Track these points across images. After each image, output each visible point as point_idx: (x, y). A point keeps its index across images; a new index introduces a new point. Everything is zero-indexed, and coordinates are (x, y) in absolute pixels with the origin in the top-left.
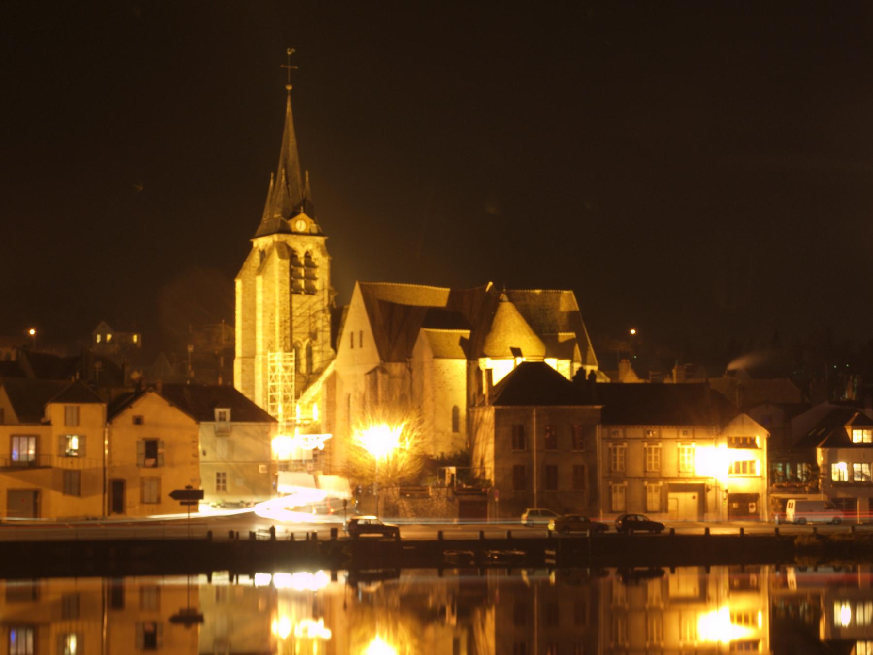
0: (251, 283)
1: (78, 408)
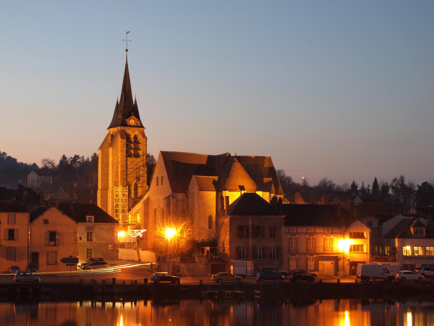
0: (106, 151)
1: (15, 215)
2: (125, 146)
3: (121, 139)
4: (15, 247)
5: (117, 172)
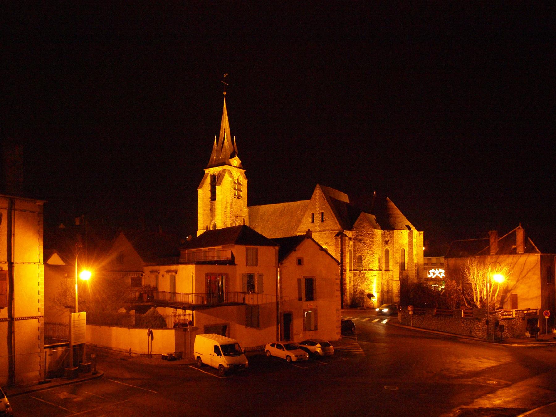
0: (206, 191)
1: (257, 249)
3: (230, 178)
4: (259, 305)
5: (226, 212)
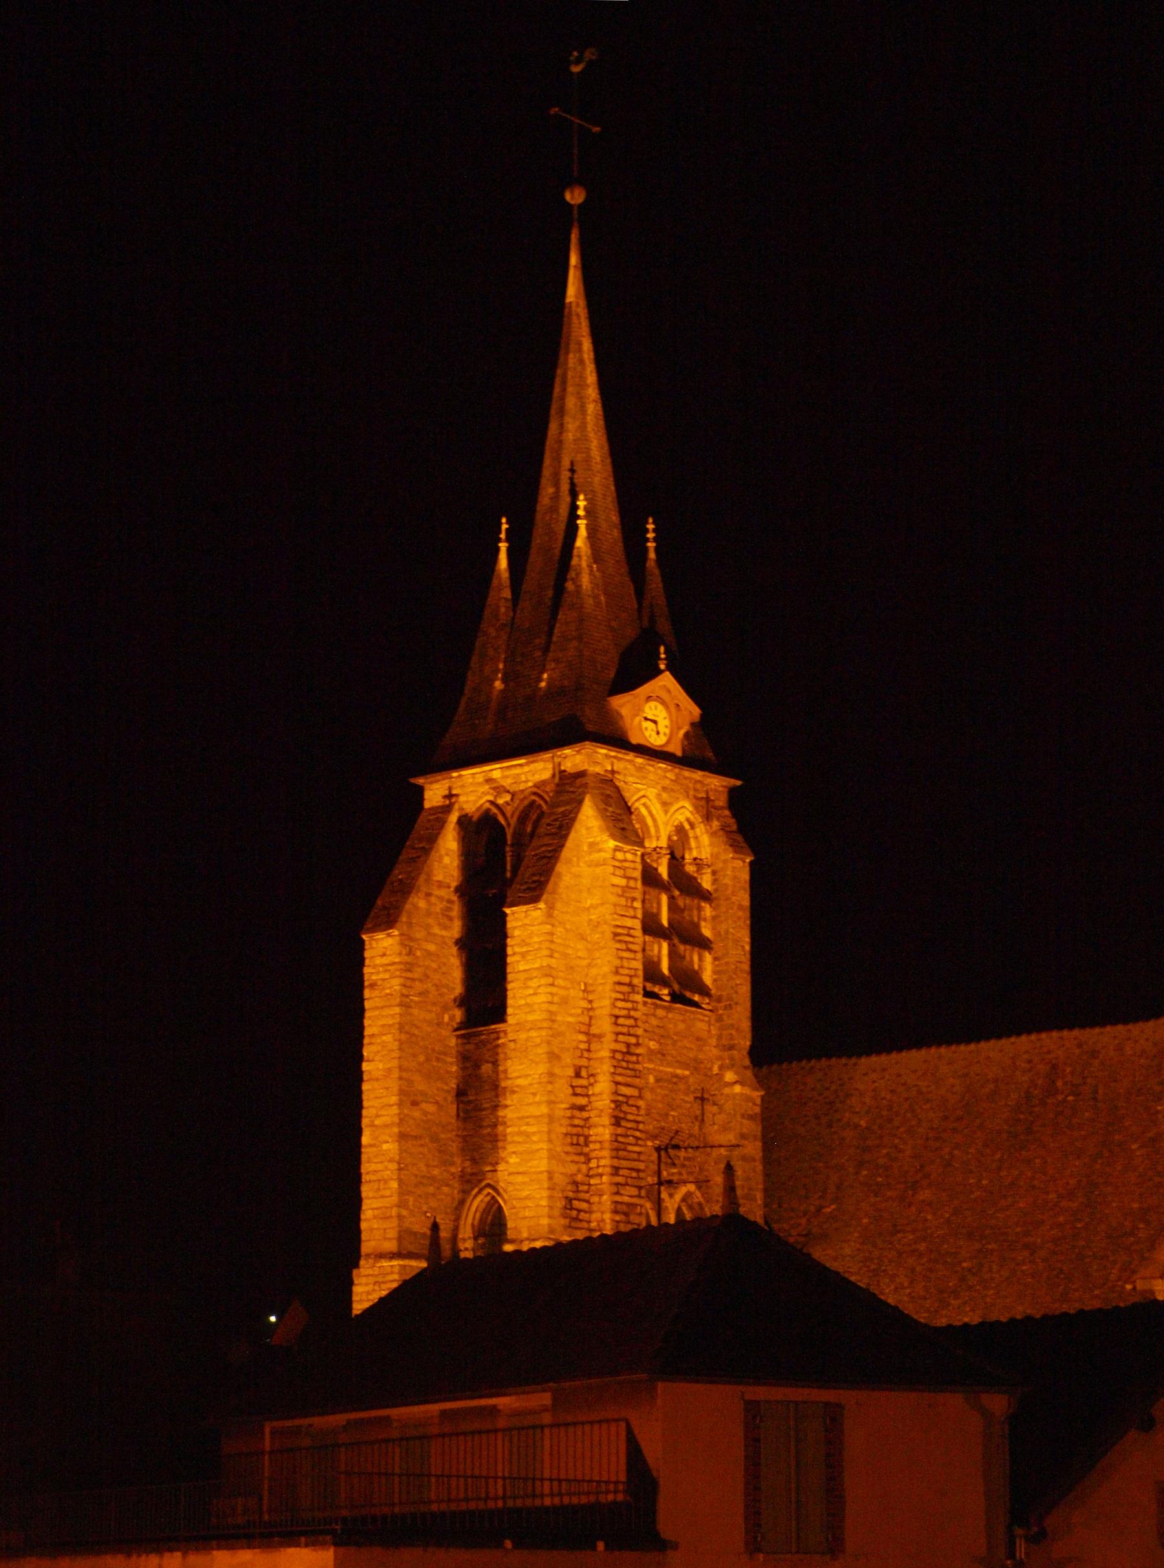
0: (432, 947)
1: (833, 1415)
2: (634, 899)
3: (612, 843)
5: (582, 1108)
